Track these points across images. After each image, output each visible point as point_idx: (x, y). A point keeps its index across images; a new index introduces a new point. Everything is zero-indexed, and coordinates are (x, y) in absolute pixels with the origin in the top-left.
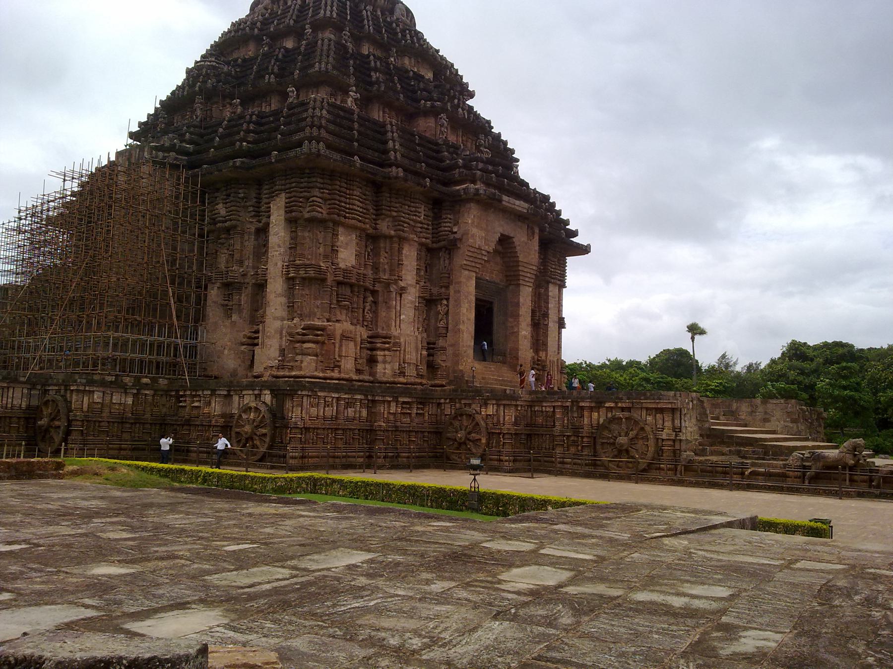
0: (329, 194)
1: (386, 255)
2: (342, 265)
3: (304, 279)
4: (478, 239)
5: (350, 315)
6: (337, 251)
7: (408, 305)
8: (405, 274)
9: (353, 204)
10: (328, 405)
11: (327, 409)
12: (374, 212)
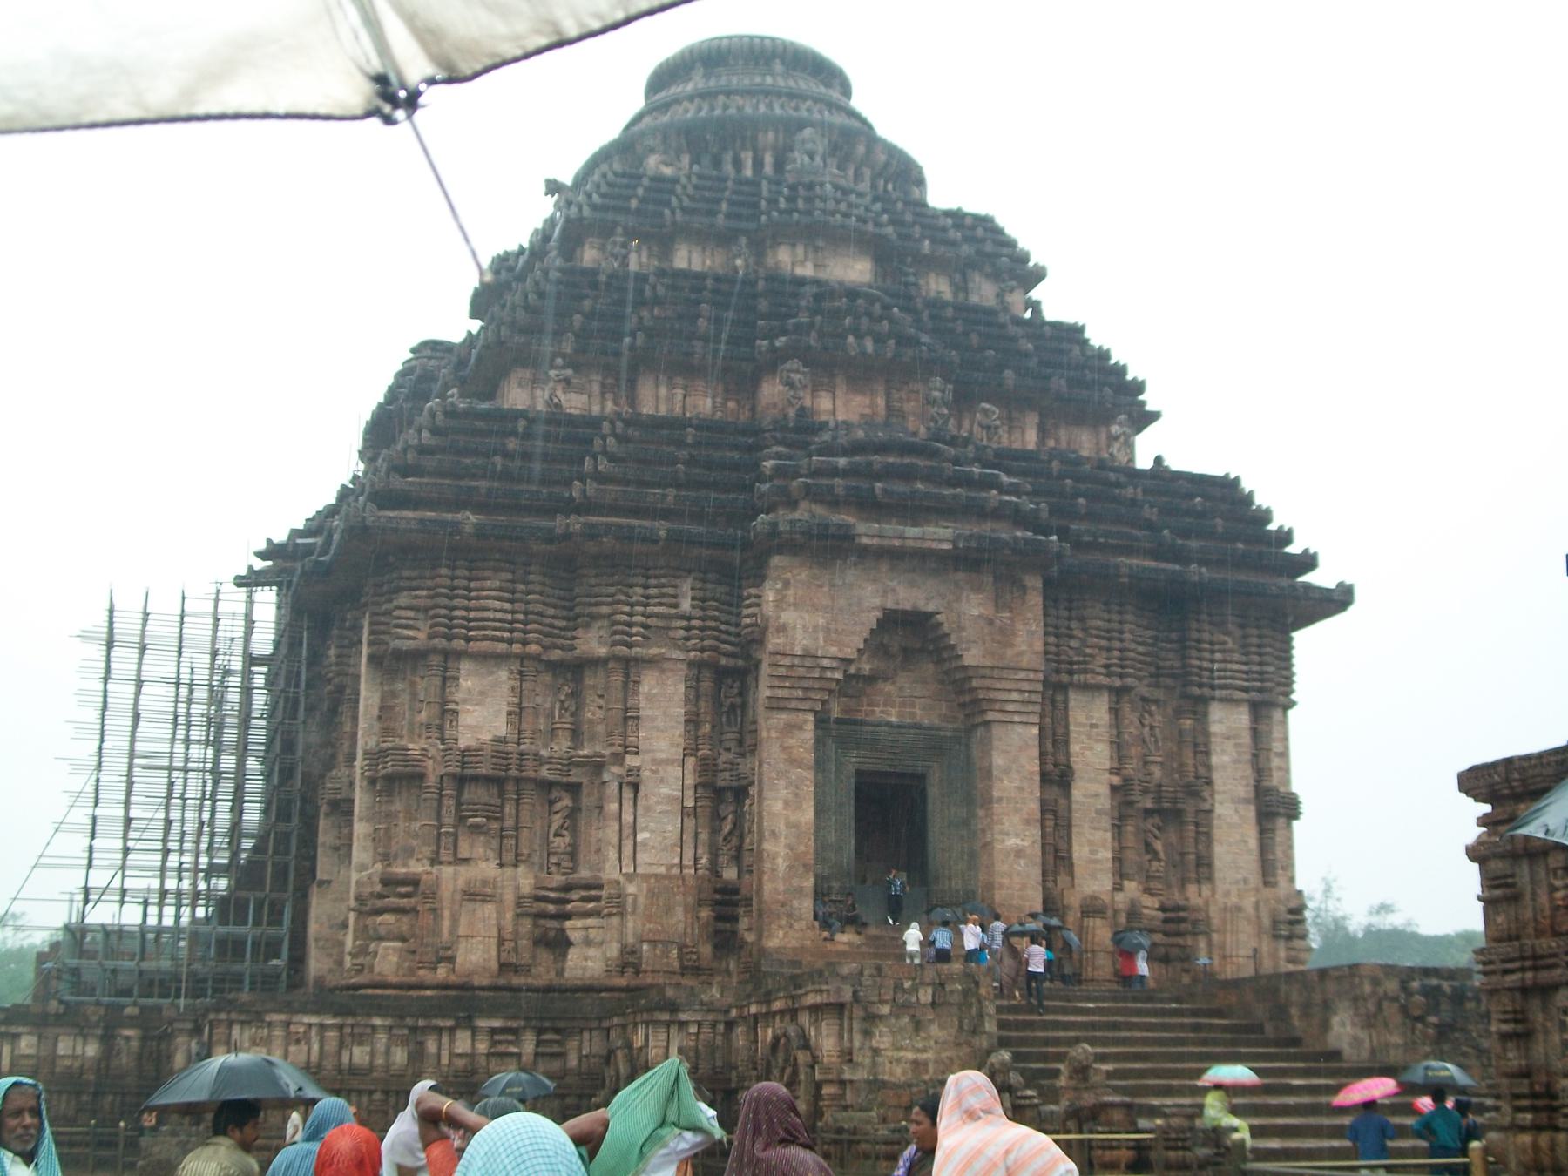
0: (429, 597)
1: (601, 702)
2: (462, 744)
3: (390, 779)
4: (799, 634)
5: (495, 843)
6: (456, 712)
7: (659, 808)
8: (646, 739)
9: (488, 609)
10: (298, 1041)
11: (292, 1048)
12: (565, 613)
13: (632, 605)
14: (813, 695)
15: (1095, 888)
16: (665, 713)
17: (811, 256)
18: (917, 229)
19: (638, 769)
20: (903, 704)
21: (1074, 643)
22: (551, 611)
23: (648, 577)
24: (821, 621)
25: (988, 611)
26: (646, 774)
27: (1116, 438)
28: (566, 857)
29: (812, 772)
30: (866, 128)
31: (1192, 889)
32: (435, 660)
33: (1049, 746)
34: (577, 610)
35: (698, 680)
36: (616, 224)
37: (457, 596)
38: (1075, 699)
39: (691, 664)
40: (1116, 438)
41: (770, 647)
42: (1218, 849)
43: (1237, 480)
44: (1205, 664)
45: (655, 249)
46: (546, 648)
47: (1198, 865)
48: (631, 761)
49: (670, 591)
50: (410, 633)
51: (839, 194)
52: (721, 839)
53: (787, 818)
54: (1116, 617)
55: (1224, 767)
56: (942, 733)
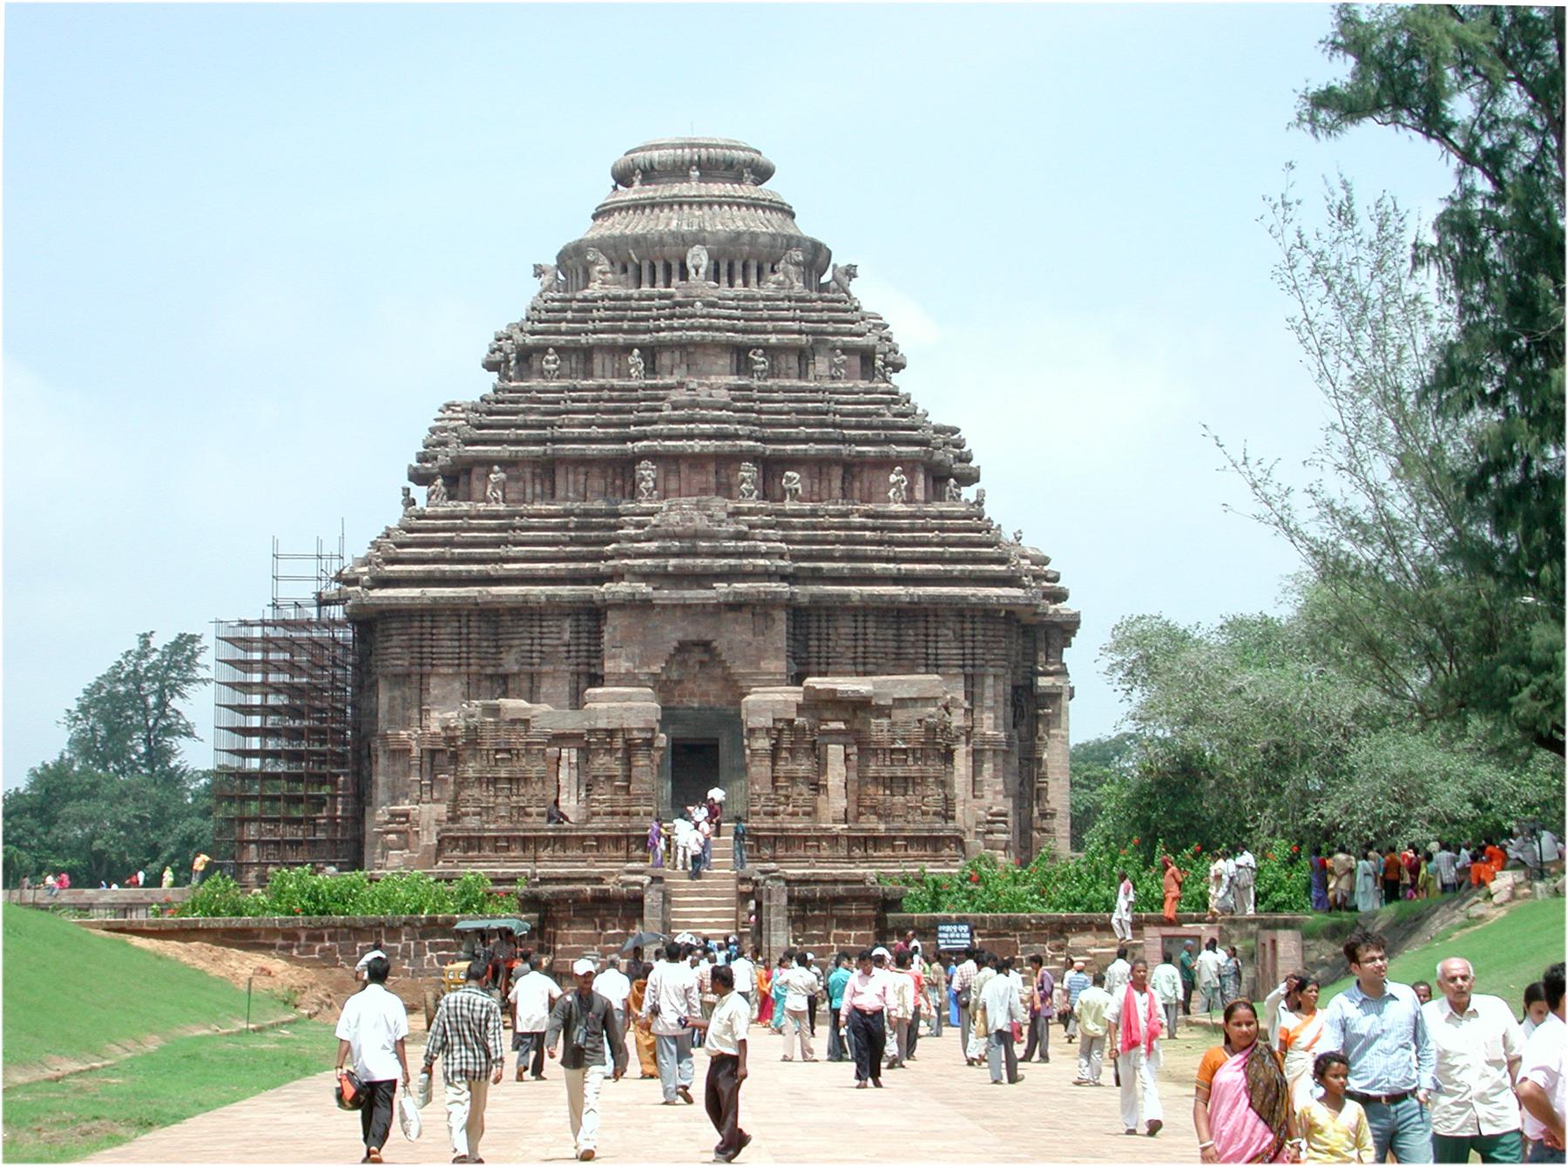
6: (428, 710)
13: (533, 639)
17: (685, 360)
21: (830, 644)
22: (485, 644)
23: (541, 620)
24: (637, 651)
25: (748, 637)
27: (894, 484)
32: (415, 678)
35: (578, 683)
39: (572, 674)
41: (606, 670)
45: (582, 357)
46: (482, 667)
49: (554, 629)
50: (399, 662)
54: (860, 624)
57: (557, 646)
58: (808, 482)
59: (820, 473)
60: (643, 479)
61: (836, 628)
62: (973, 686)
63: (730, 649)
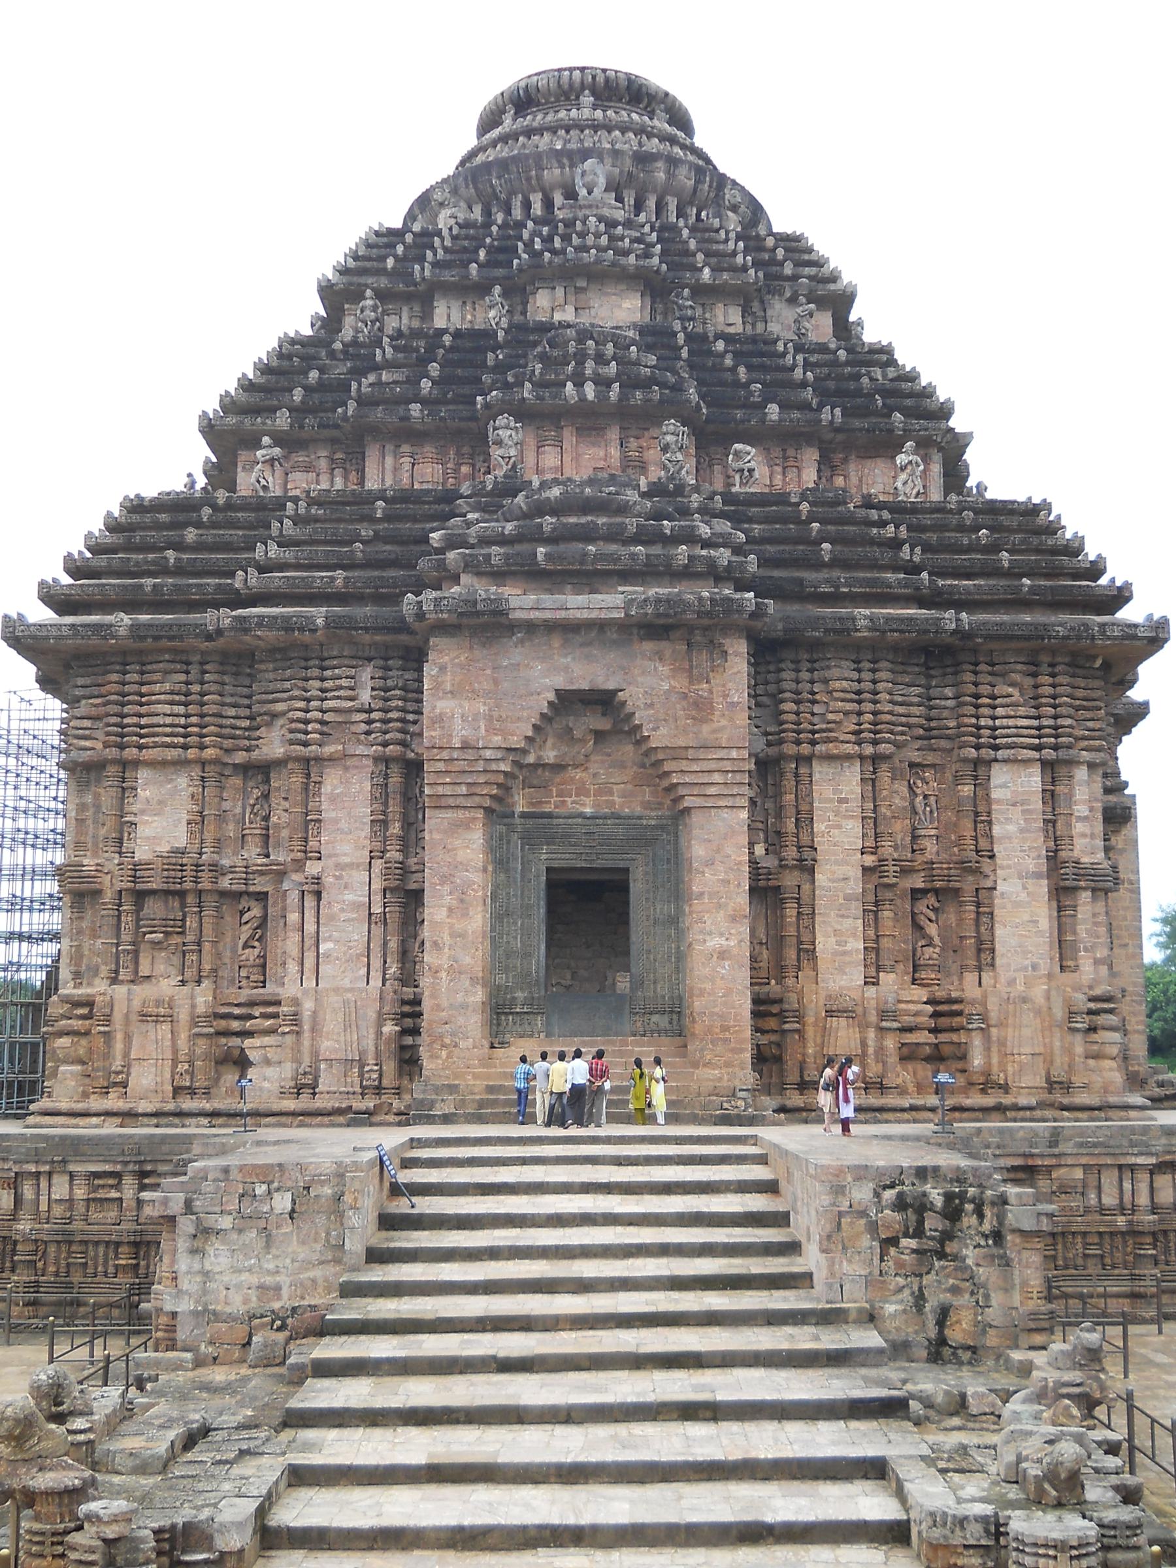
1: (286, 804)
2: (138, 857)
5: (176, 960)
7: (343, 916)
8: (327, 843)
12: (246, 712)
14: (478, 790)
15: (843, 983)
16: (349, 813)
17: (571, 298)
18: (700, 257)
19: (317, 880)
20: (598, 793)
22: (232, 712)
23: (324, 669)
25: (680, 683)
26: (328, 880)
27: (903, 469)
28: (255, 970)
29: (480, 874)
30: (691, 158)
31: (970, 978)
32: (112, 770)
33: (790, 826)
34: (255, 708)
36: (367, 286)
37: (130, 703)
38: (819, 771)
39: (377, 759)
40: (903, 469)
42: (999, 931)
43: (1046, 506)
44: (982, 722)
45: (417, 308)
47: (979, 951)
48: (312, 868)
49: (344, 682)
50: (88, 744)
51: (602, 227)
52: (417, 945)
53: (451, 926)
54: (866, 675)
55: (1010, 838)
56: (645, 822)
57: (349, 711)
58: (766, 471)
59: (785, 458)
60: (499, 443)
61: (826, 681)
62: (1053, 783)
63: (651, 706)
